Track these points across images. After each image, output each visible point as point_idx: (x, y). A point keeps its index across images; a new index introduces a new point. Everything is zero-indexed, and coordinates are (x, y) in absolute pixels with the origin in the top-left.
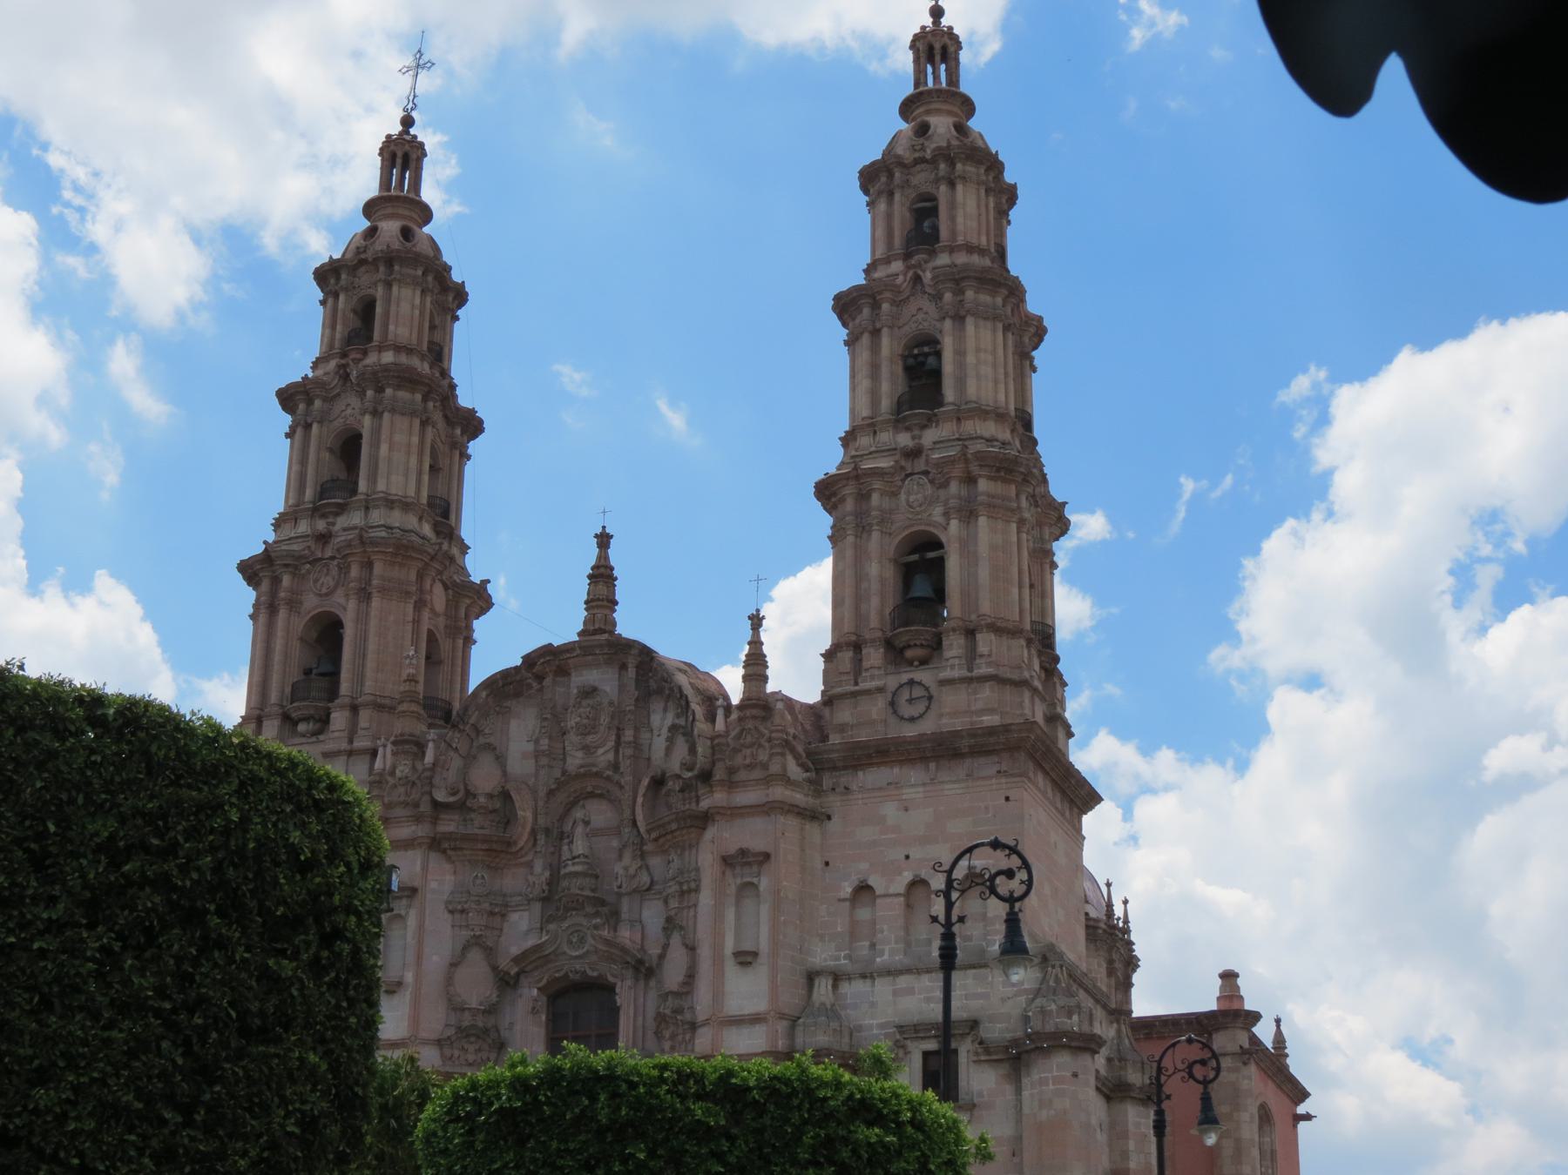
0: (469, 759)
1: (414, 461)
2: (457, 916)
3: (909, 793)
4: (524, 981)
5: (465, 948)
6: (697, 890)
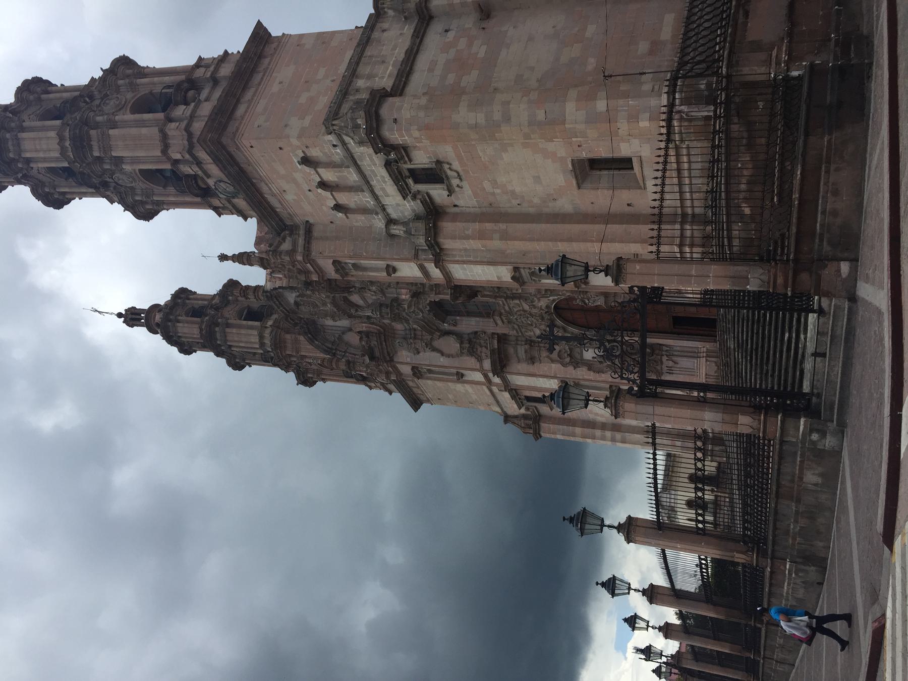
0: (348, 344)
1: (243, 331)
3: (275, 191)
4: (442, 328)
5: (434, 349)
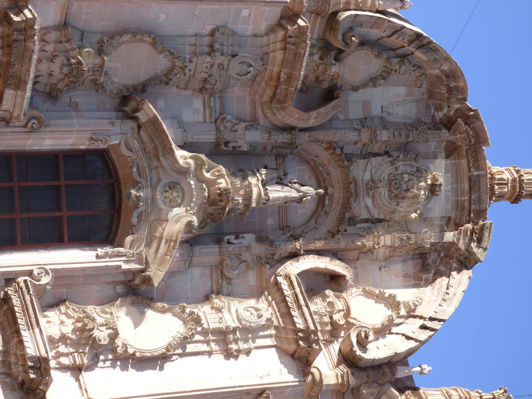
2: (207, 40)
6: (229, 355)
